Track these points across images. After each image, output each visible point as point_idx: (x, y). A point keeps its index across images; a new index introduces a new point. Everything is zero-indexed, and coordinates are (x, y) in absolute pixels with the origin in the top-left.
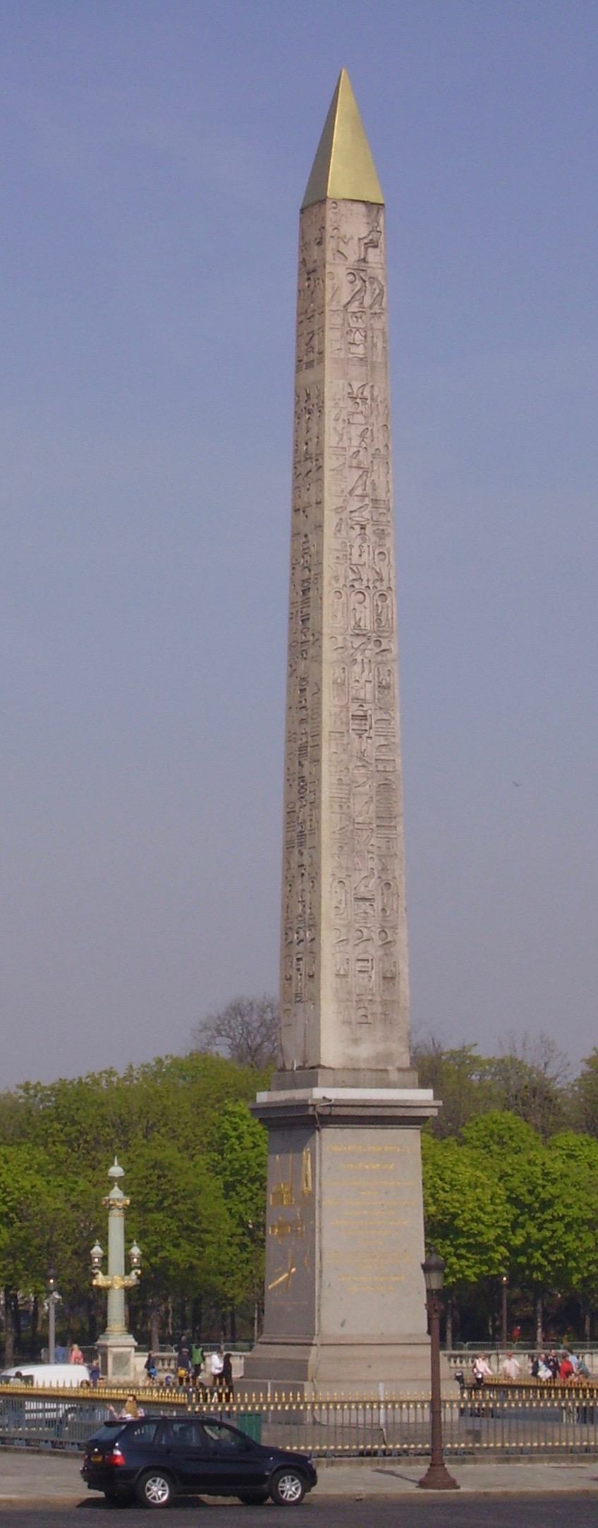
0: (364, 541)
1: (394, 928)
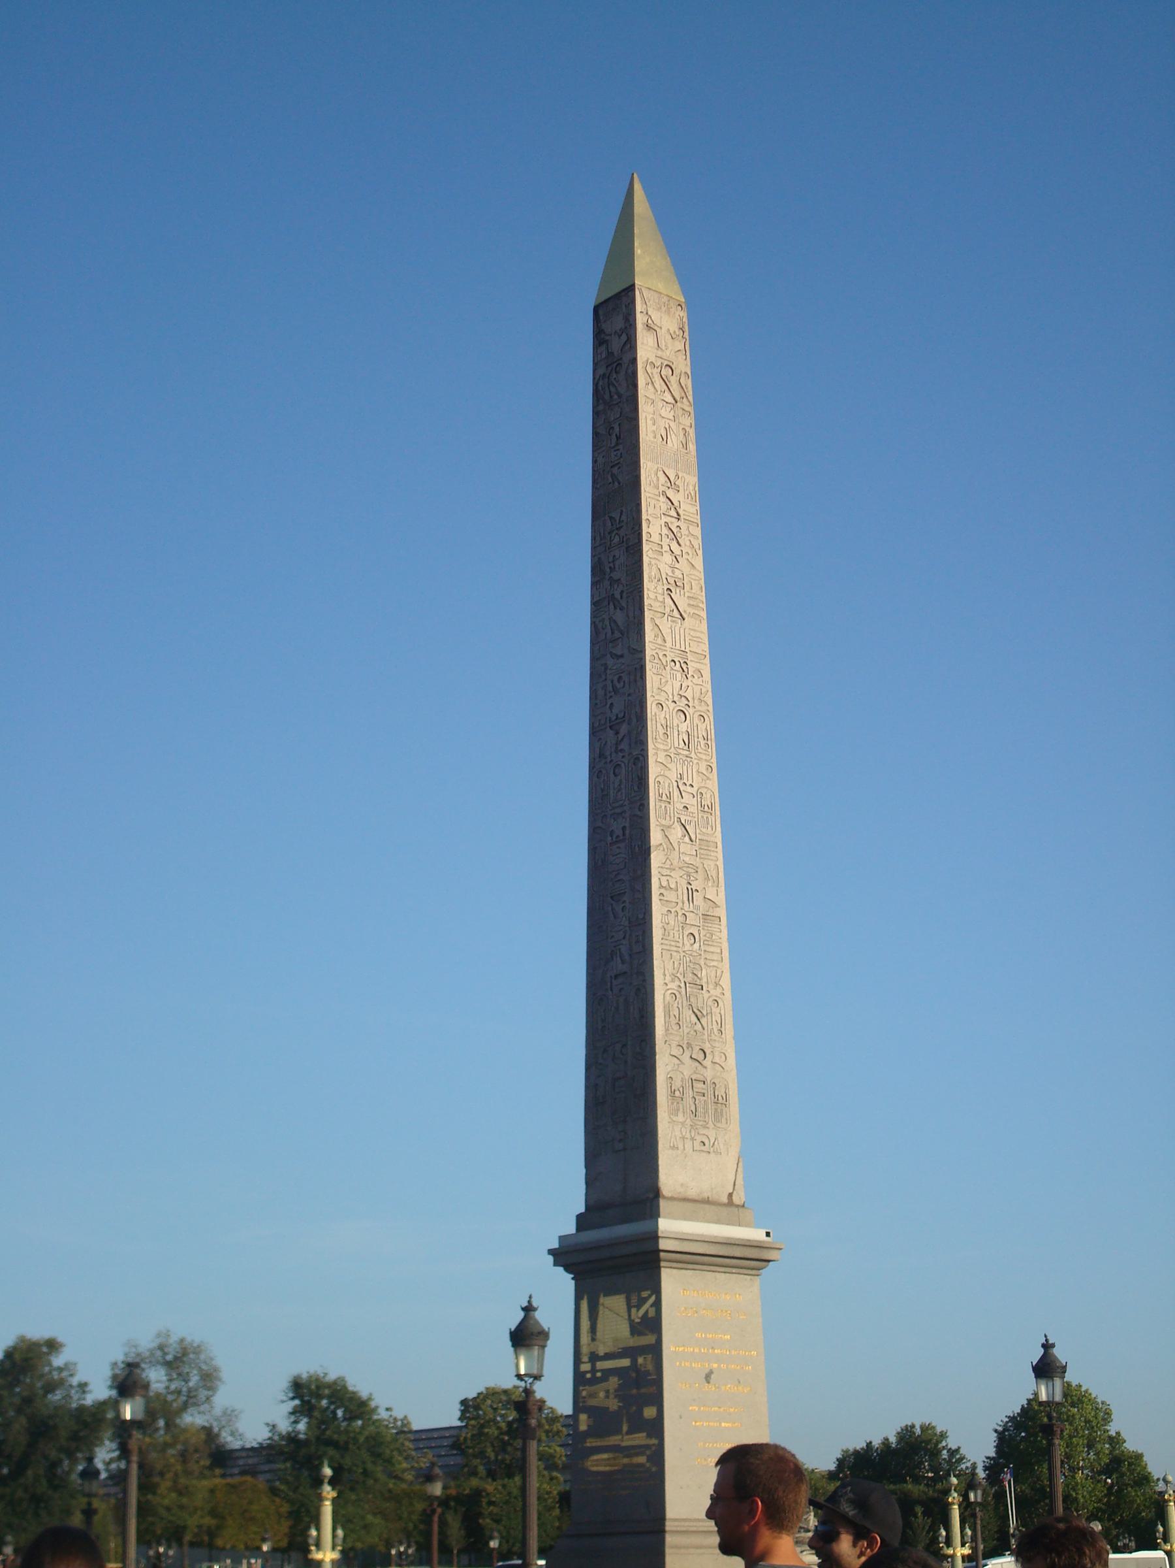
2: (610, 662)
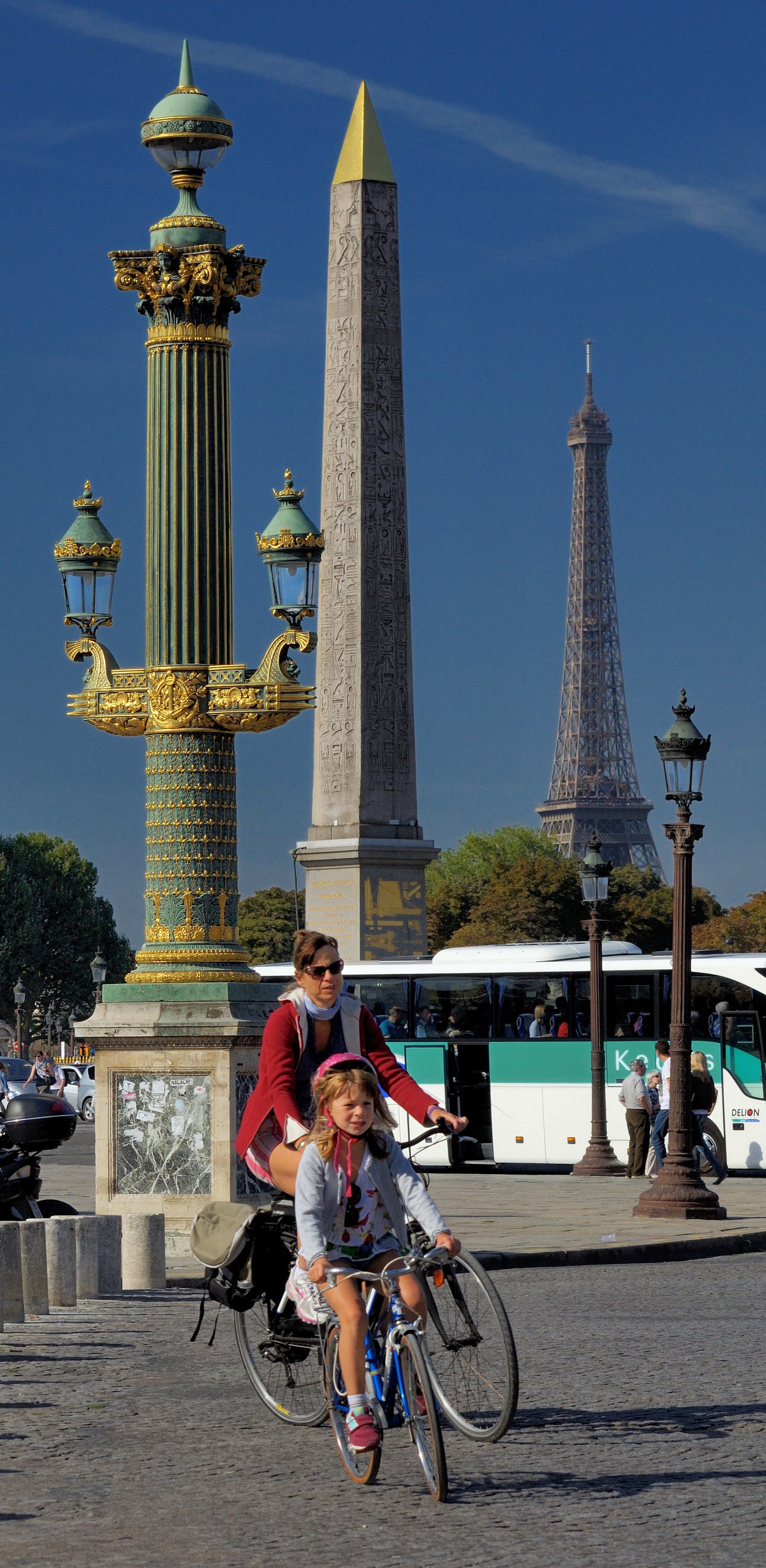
0: (344, 434)
1: (353, 719)
2: (379, 453)
